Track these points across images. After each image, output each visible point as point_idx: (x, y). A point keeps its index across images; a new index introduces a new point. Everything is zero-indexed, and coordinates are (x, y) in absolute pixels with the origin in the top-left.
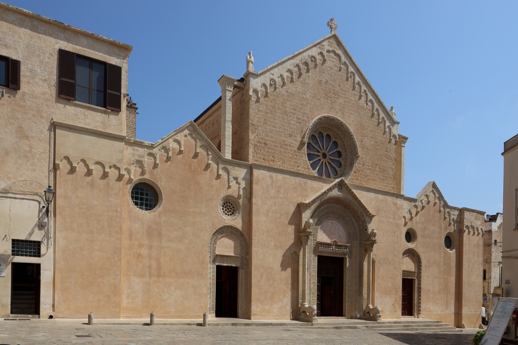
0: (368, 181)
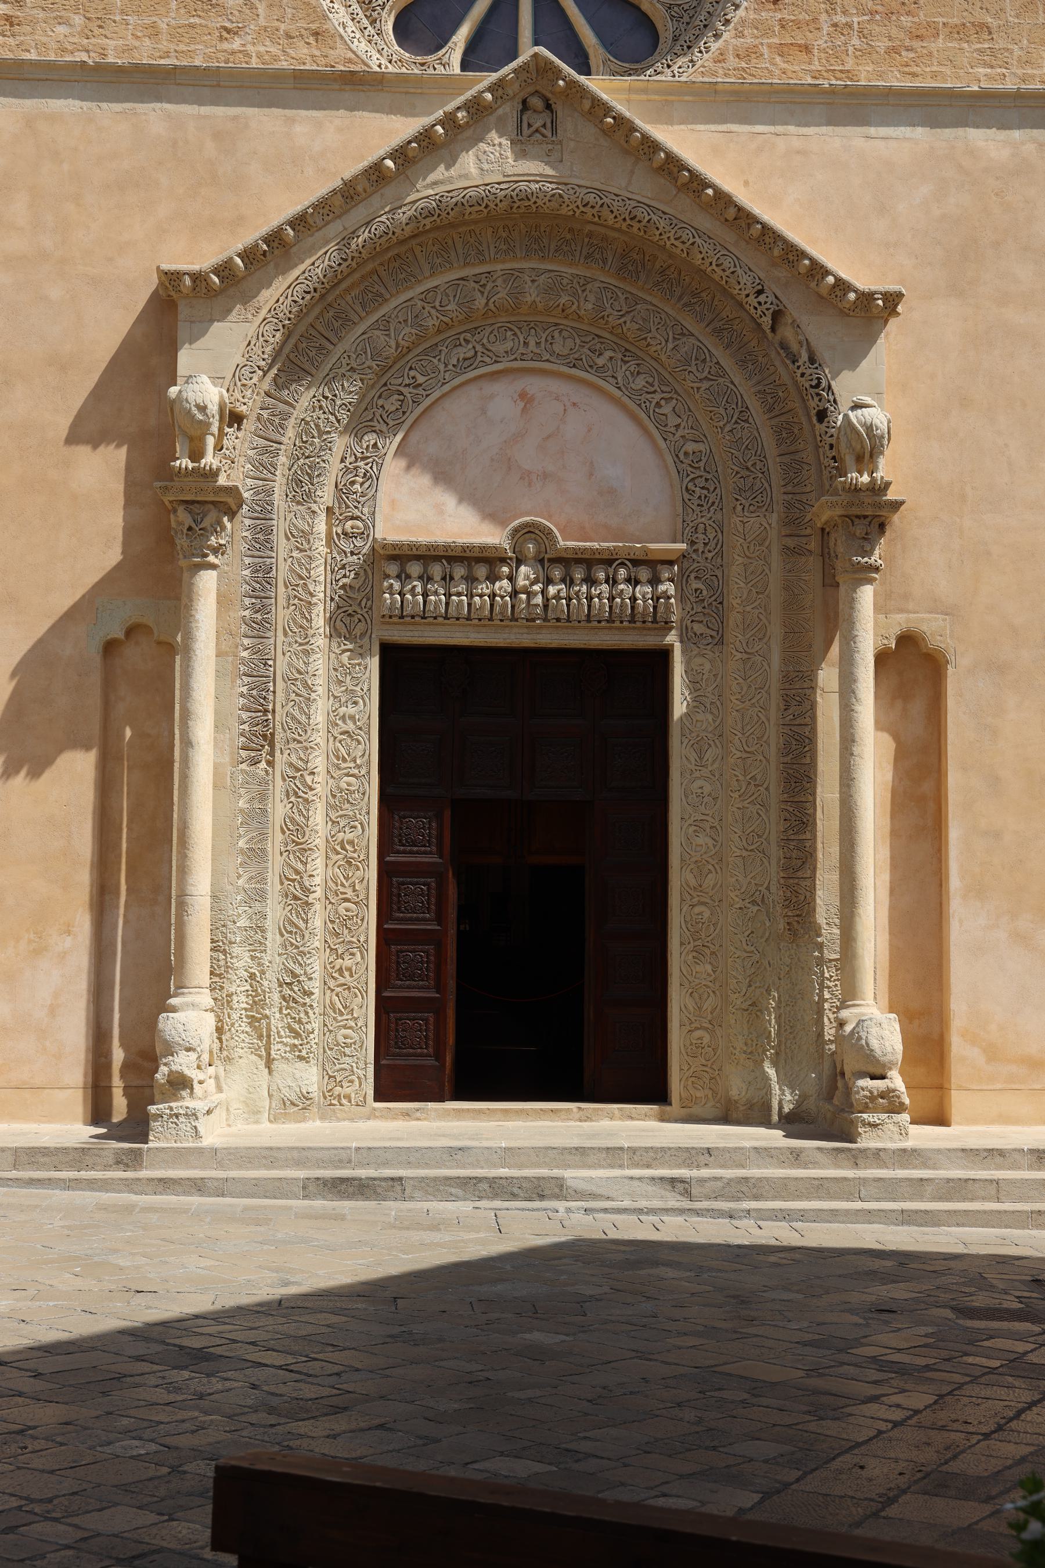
0: (916, 44)
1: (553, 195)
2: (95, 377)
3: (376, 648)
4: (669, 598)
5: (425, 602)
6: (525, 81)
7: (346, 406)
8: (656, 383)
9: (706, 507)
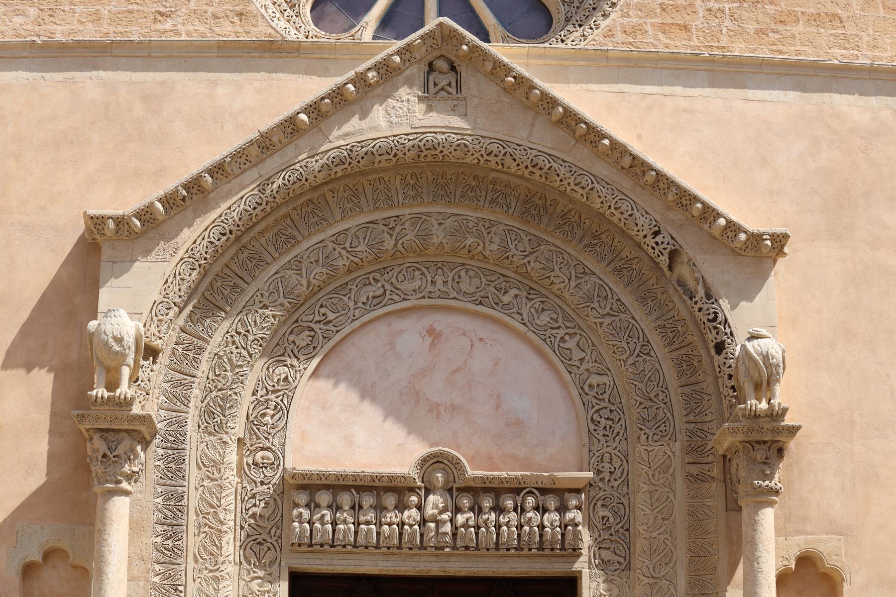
0: (781, 27)
1: (459, 145)
2: (25, 315)
3: (285, 575)
4: (577, 525)
5: (334, 531)
6: (431, 46)
7: (258, 341)
8: (560, 320)
9: (611, 437)
